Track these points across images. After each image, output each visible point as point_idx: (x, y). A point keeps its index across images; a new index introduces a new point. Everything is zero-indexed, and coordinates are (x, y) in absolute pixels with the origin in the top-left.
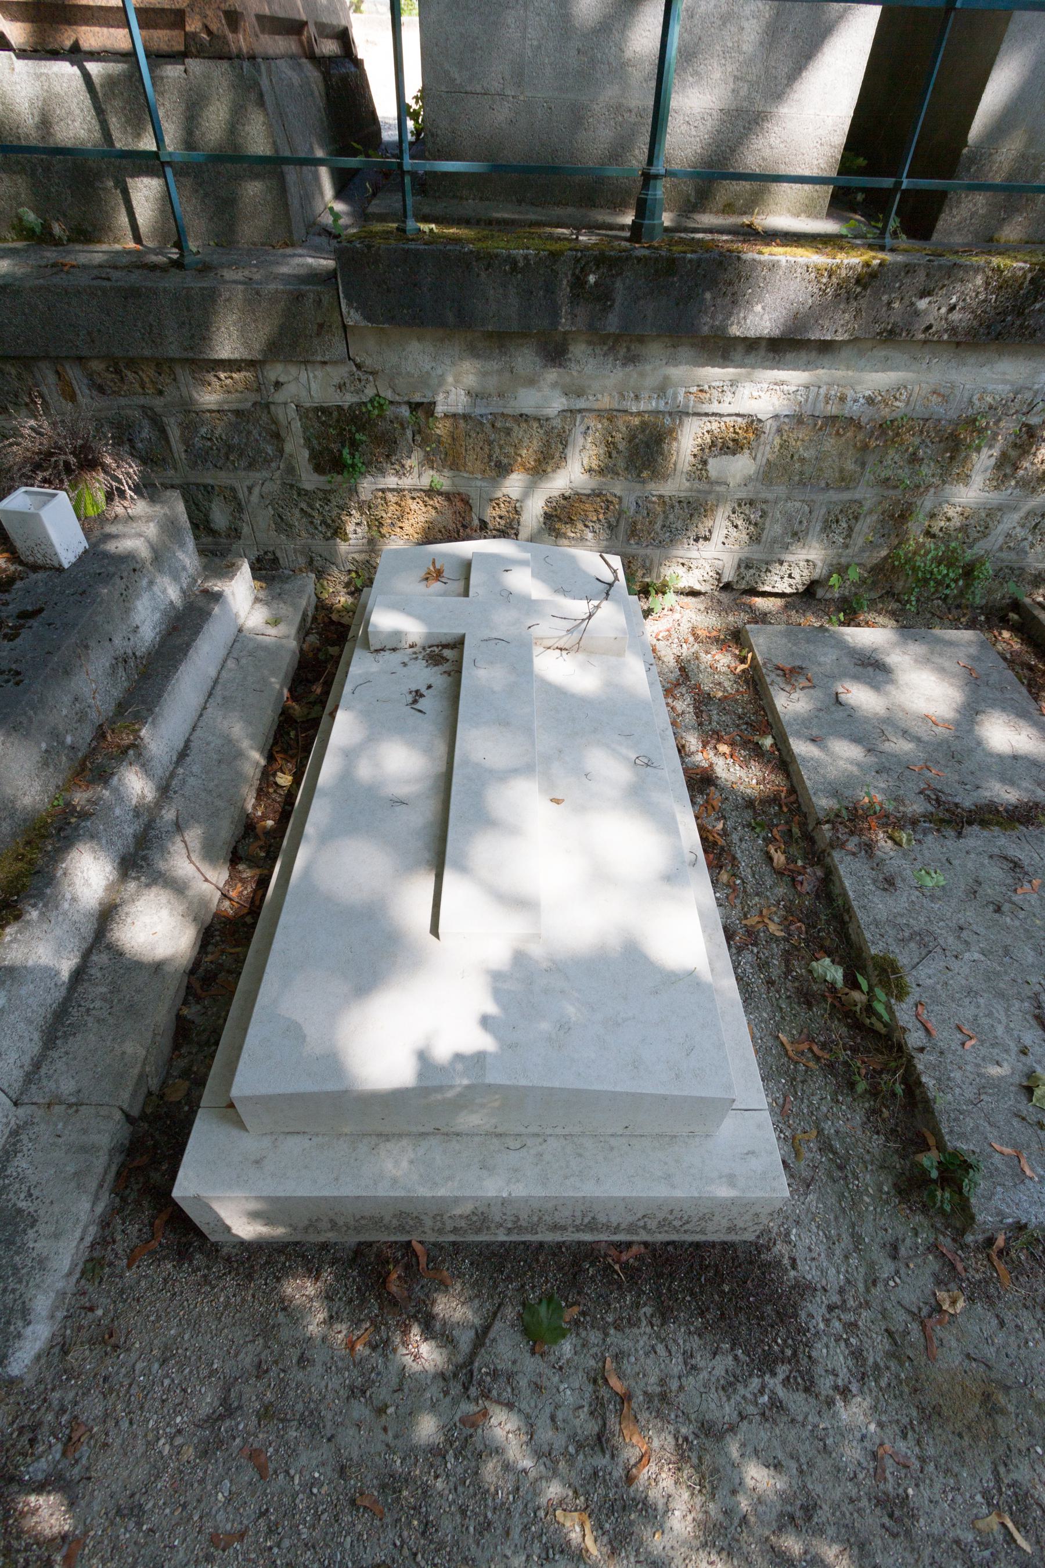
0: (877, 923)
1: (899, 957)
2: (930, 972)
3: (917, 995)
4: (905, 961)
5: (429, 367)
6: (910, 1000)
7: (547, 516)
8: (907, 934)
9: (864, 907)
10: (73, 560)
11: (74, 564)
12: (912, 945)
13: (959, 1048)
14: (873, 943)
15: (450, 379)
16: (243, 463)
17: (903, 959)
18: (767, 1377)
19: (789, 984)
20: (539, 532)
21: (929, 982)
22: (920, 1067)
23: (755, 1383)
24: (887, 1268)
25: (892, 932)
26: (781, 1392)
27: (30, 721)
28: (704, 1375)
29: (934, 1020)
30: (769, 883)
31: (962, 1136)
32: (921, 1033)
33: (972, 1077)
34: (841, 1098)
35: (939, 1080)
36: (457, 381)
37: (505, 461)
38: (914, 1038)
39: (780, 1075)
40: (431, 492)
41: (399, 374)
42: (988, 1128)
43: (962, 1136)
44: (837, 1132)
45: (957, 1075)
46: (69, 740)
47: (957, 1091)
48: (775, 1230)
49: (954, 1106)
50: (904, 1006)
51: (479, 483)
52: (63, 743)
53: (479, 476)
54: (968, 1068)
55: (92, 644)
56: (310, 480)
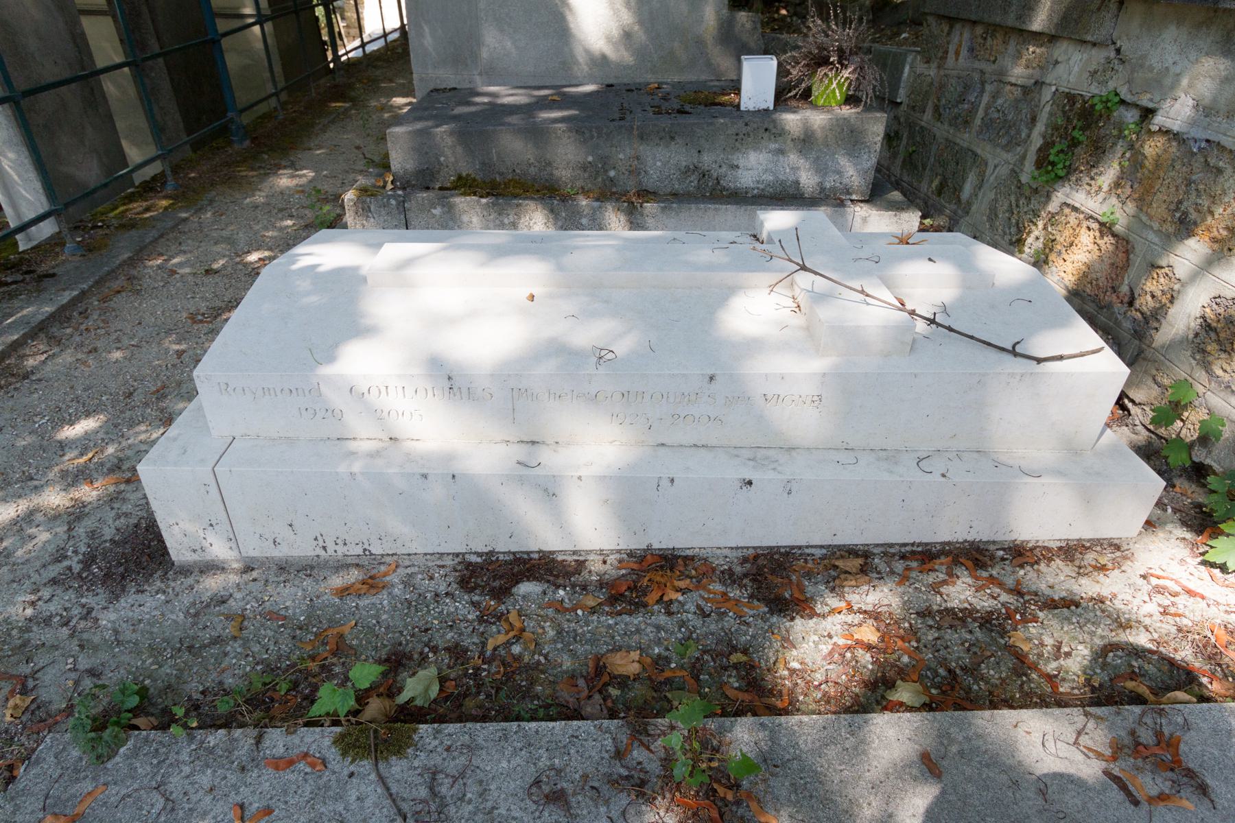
0: (472, 748)
1: (404, 762)
2: (368, 803)
3: (337, 768)
4: (396, 770)
5: (1171, 61)
6: (333, 754)
7: (1207, 326)
8: (444, 790)
9: (505, 737)
10: (751, 109)
11: (748, 111)
12: (423, 792)
13: (239, 799)
14: (438, 732)
15: (1185, 82)
16: (1004, 141)
17: (397, 768)
18: (81, 557)
19: (419, 647)
20: (1181, 342)
21: (353, 795)
22: (238, 733)
23: (83, 549)
24: (84, 663)
25: (453, 766)
26: (66, 563)
27: (592, 137)
28: (111, 522)
29: (292, 777)
30: (580, 649)
31: (135, 753)
32: (279, 751)
33: (194, 798)
34: (259, 668)
35: (211, 751)
36: (1190, 86)
37: (1193, 215)
38: (277, 741)
39: (308, 617)
40: (1106, 228)
41: (1142, 66)
42: (124, 792)
43: (135, 753)
44: (226, 654)
45: (205, 779)
46: (612, 173)
47: (187, 770)
48: (173, 584)
49: (172, 757)
50: (327, 742)
51: (1152, 236)
52: (606, 171)
53: (1156, 226)
54: (208, 799)
55: (678, 140)
56: (1028, 173)
